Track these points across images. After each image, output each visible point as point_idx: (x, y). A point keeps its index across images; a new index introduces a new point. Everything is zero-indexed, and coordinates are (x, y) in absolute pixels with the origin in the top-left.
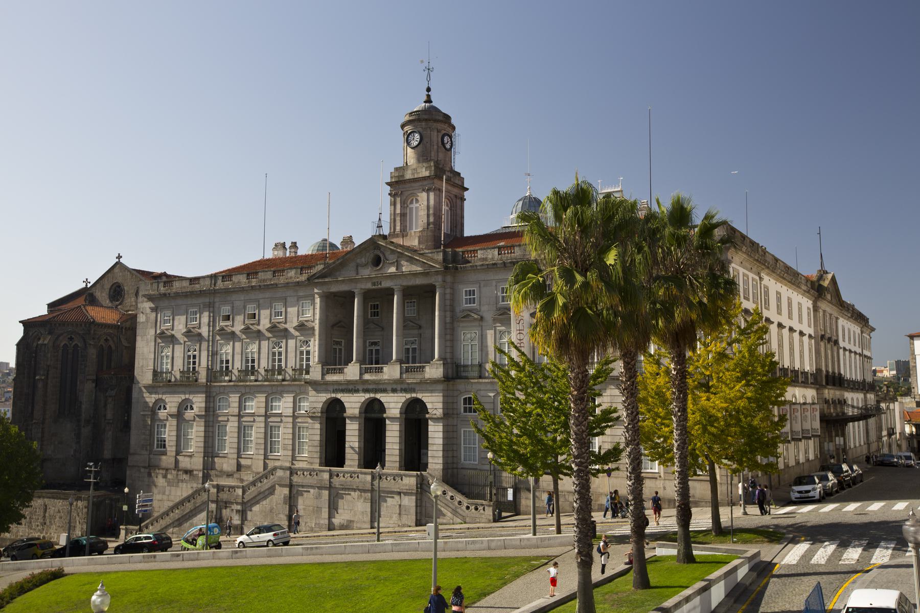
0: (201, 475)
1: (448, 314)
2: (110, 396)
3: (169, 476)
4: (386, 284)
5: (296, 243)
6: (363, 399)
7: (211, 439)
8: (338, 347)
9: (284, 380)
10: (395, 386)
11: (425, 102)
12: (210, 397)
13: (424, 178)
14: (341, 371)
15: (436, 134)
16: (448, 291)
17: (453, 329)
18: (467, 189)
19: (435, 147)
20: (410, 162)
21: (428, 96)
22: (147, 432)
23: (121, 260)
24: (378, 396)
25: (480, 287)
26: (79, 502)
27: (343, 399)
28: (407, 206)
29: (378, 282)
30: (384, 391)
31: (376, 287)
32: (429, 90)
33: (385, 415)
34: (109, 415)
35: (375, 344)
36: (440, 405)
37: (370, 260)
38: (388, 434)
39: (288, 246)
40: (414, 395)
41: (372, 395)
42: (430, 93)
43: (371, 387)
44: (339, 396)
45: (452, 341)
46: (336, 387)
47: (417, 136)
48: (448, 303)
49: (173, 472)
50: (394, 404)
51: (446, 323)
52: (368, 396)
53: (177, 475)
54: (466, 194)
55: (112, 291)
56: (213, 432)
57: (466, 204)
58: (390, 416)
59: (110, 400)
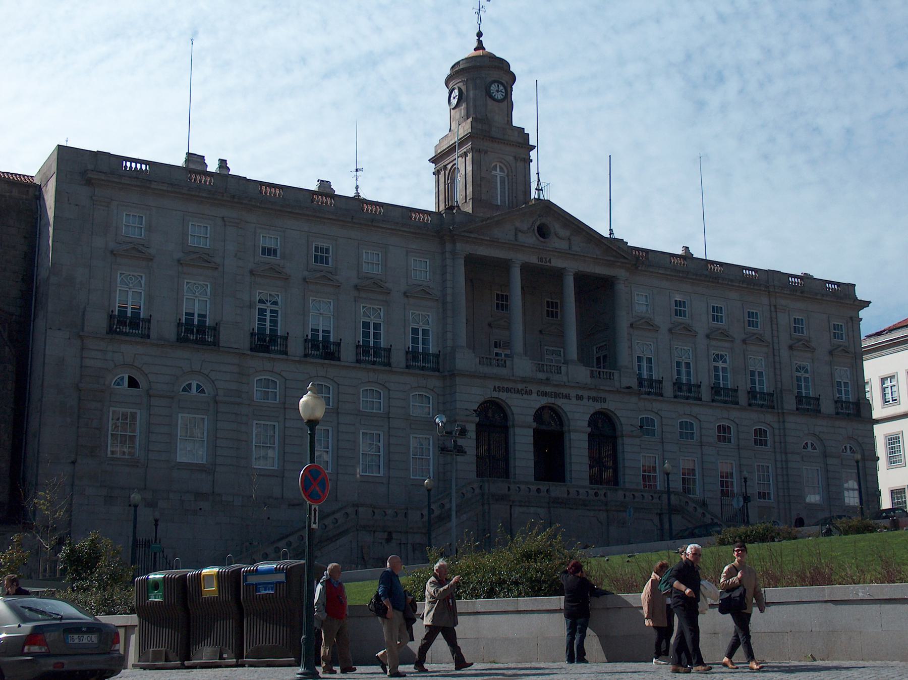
4: (557, 263)
6: (538, 406)
10: (580, 393)
11: (475, 50)
24: (560, 402)
27: (509, 402)
29: (546, 259)
30: (567, 397)
31: (543, 264)
32: (480, 34)
37: (536, 229)
40: (604, 406)
42: (481, 39)
43: (548, 389)
44: (503, 396)
46: (498, 384)
52: (544, 401)
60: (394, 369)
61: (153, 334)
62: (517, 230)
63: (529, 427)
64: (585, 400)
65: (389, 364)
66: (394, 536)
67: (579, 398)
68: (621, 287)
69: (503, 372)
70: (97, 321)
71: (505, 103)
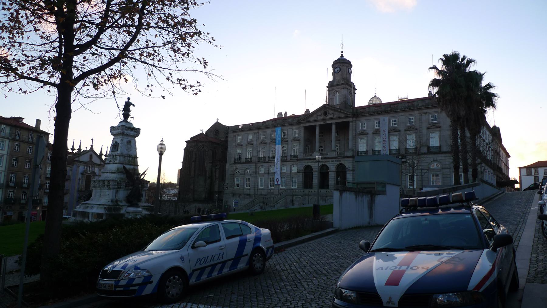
0: (253, 196)
1: (354, 132)
2: (218, 168)
3: (241, 197)
4: (329, 122)
5: (286, 113)
7: (257, 183)
8: (307, 148)
9: (286, 160)
11: (341, 57)
12: (257, 167)
13: (342, 84)
14: (311, 155)
15: (346, 68)
16: (354, 124)
17: (356, 138)
18: (356, 90)
19: (346, 73)
20: (336, 78)
21: (342, 55)
22: (232, 181)
23: (219, 121)
24: (326, 163)
25: (367, 122)
26: (209, 205)
28: (334, 95)
30: (329, 162)
32: (342, 52)
33: (329, 171)
34: (217, 175)
35: (321, 147)
36: (351, 166)
38: (330, 177)
39: (283, 114)
40: (341, 163)
41: (324, 163)
42: (343, 53)
44: (310, 164)
45: (355, 142)
47: (338, 69)
48: (354, 128)
49: (242, 195)
50: (332, 166)
51: (353, 136)
53: (244, 196)
54: (356, 91)
55: (214, 132)
56: (258, 180)
57: (356, 95)
58: (331, 171)
59: (217, 170)
60: (287, 161)
61: (242, 162)
62: (318, 116)
63: (317, 172)
64: (334, 162)
65: (286, 160)
66: (267, 204)
67: (332, 161)
68: (351, 124)
69: (311, 157)
70: (233, 160)
71: (340, 72)
